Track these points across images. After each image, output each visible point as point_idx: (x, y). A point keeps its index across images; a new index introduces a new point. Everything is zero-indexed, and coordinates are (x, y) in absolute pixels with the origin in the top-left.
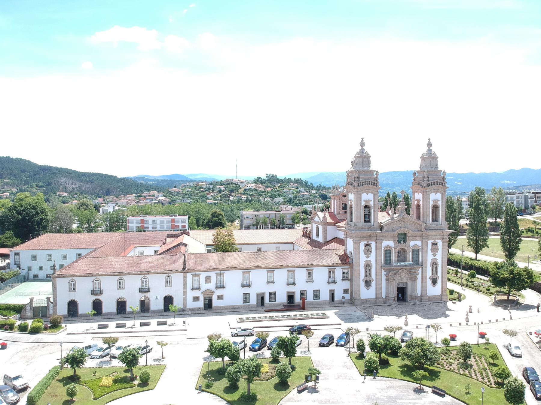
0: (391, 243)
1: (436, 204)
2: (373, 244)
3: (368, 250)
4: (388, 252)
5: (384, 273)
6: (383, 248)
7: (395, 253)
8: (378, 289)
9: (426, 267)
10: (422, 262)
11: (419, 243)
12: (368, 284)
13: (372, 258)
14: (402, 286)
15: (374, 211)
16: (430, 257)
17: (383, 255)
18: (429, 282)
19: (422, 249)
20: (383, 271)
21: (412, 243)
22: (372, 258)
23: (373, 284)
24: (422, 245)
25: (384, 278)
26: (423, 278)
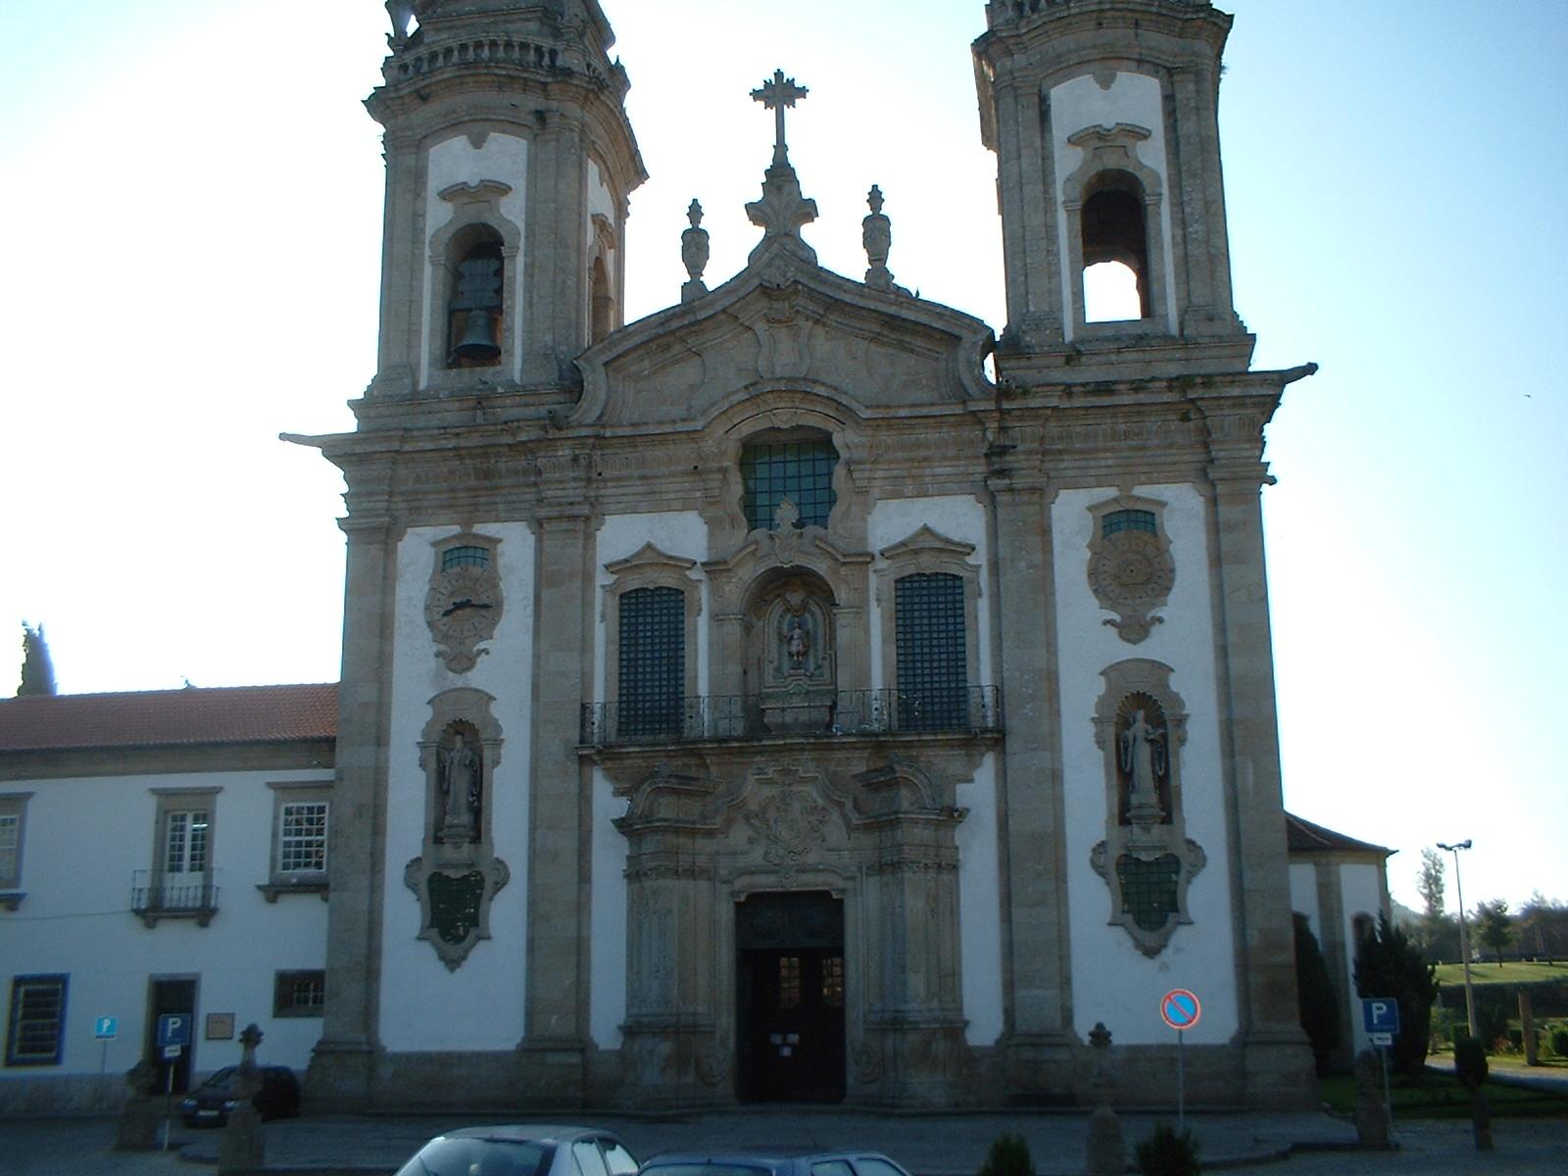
0: (685, 535)
1: (1112, 161)
2: (515, 546)
3: (465, 606)
4: (651, 614)
5: (607, 802)
6: (603, 579)
7: (717, 618)
8: (558, 949)
9: (1051, 742)
10: (998, 690)
11: (960, 518)
12: (454, 909)
13: (505, 667)
15: (530, 268)
16: (1086, 647)
17: (602, 636)
18: (1091, 899)
19: (995, 567)
20: (602, 788)
21: (889, 523)
22: (505, 667)
23: (506, 914)
24: (993, 534)
25: (609, 856)
26: (1030, 861)
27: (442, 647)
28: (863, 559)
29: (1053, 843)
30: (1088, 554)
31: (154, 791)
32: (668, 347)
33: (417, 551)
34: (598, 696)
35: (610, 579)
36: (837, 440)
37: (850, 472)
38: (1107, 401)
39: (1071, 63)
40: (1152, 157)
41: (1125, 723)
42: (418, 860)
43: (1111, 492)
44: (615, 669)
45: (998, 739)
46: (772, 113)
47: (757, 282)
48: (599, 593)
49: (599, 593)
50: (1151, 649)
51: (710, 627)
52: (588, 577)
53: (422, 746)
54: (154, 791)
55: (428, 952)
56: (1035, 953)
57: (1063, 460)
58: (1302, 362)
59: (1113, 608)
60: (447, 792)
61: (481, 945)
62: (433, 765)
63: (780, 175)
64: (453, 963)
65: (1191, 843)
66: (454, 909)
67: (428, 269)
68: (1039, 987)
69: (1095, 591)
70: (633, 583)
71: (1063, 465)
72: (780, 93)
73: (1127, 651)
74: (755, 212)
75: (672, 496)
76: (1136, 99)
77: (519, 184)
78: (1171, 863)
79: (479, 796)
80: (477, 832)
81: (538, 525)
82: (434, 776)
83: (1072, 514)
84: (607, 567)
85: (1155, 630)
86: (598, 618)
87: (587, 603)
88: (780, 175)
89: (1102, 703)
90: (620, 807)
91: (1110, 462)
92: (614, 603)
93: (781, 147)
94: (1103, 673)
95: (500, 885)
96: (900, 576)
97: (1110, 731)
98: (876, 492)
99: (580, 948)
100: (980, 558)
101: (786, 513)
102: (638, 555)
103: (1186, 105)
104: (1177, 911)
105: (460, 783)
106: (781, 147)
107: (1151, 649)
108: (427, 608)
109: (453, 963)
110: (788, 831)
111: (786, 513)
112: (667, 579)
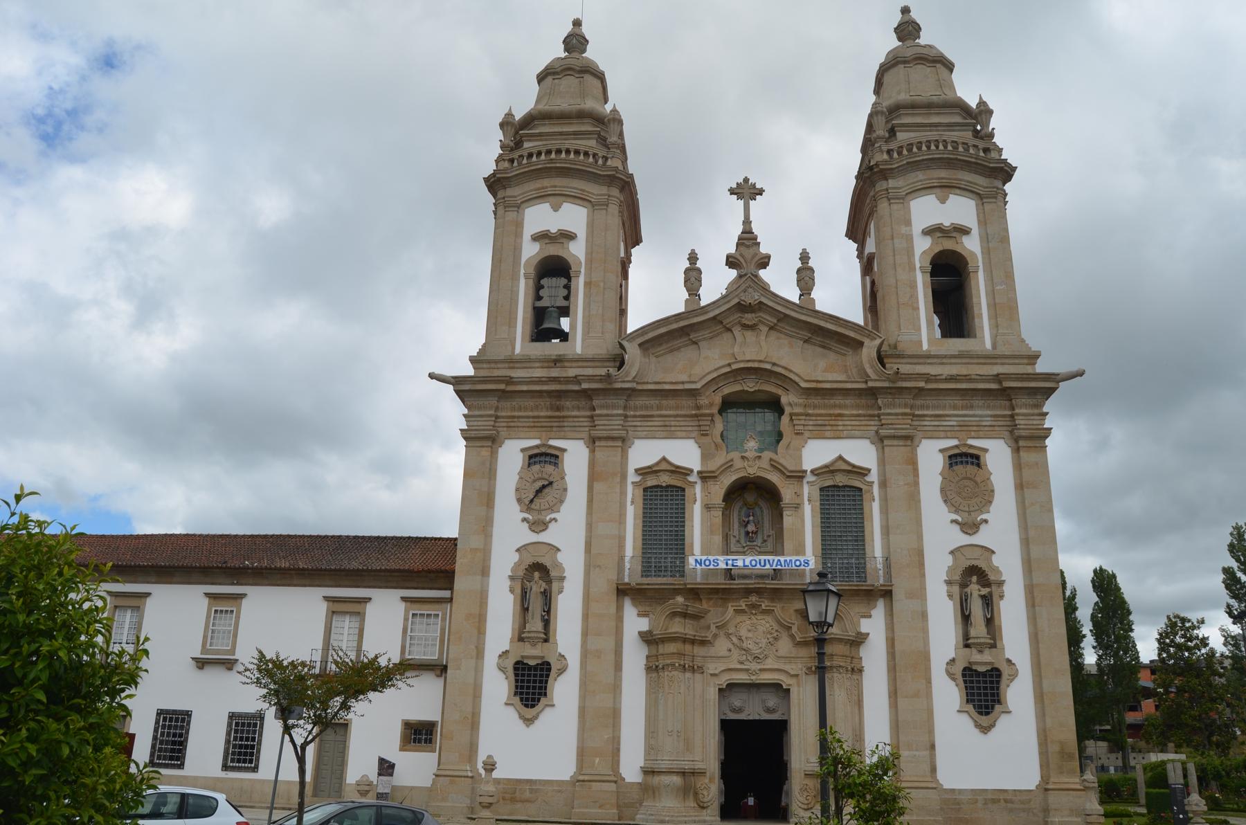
0: (685, 453)
1: (948, 245)
2: (576, 456)
3: (540, 493)
7: (707, 507)
9: (919, 594)
10: (887, 560)
11: (861, 452)
12: (531, 683)
13: (568, 533)
14: (753, 709)
15: (588, 284)
16: (940, 536)
18: (947, 695)
19: (883, 484)
21: (817, 454)
22: (568, 533)
23: (565, 690)
24: (882, 462)
26: (907, 668)
27: (526, 515)
28: (798, 476)
29: (923, 660)
30: (940, 478)
31: (326, 598)
33: (511, 456)
34: (629, 551)
35: (638, 479)
36: (784, 400)
37: (791, 420)
40: (972, 245)
41: (964, 585)
42: (507, 652)
44: (640, 533)
45: (887, 594)
46: (741, 202)
47: (736, 301)
48: (630, 488)
49: (630, 488)
50: (979, 539)
51: (702, 513)
52: (624, 477)
53: (512, 578)
54: (326, 598)
55: (511, 715)
58: (1074, 368)
59: (957, 511)
60: (527, 609)
61: (548, 710)
62: (518, 591)
63: (748, 239)
64: (529, 721)
65: (1009, 661)
66: (531, 683)
67: (522, 282)
69: (945, 501)
70: (651, 482)
72: (746, 191)
73: (966, 540)
74: (731, 262)
76: (959, 210)
77: (582, 234)
79: (548, 612)
80: (547, 636)
81: (592, 442)
82: (519, 597)
83: (931, 456)
84: (636, 470)
85: (983, 527)
86: (629, 503)
87: (623, 493)
88: (748, 239)
89: (951, 570)
90: (644, 624)
92: (640, 492)
93: (747, 222)
94: (952, 552)
95: (562, 671)
97: (956, 589)
99: (615, 715)
100: (874, 477)
102: (657, 464)
105: (536, 605)
106: (747, 222)
107: (979, 539)
108: (517, 490)
109: (529, 721)
110: (754, 648)
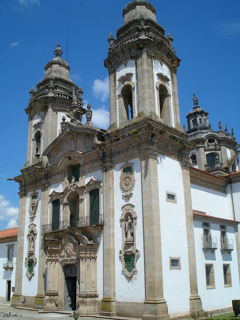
32: (57, 149)
38: (119, 142)
39: (119, 63)
43: (124, 163)
56: (108, 279)
57: (115, 158)
68: (108, 287)
71: (115, 159)
75: (59, 180)
78: (133, 255)
91: (123, 156)
96: (90, 191)
98: (86, 172)
101: (73, 180)
103: (139, 64)
104: (134, 268)
111: (73, 180)
112: (58, 197)
